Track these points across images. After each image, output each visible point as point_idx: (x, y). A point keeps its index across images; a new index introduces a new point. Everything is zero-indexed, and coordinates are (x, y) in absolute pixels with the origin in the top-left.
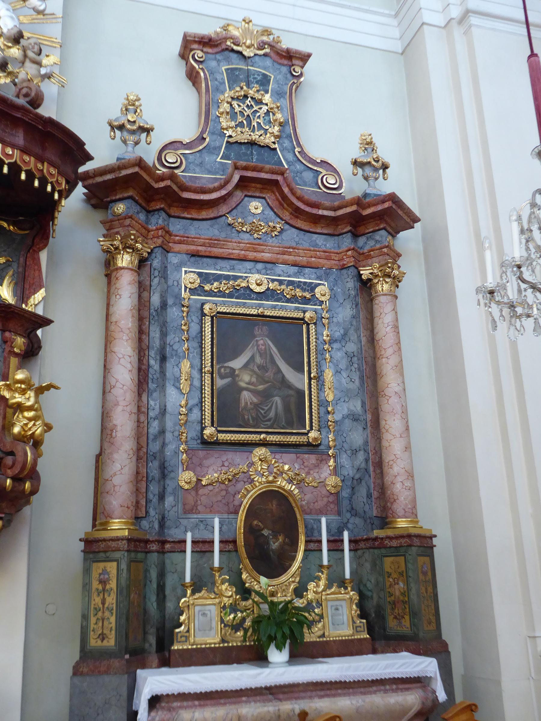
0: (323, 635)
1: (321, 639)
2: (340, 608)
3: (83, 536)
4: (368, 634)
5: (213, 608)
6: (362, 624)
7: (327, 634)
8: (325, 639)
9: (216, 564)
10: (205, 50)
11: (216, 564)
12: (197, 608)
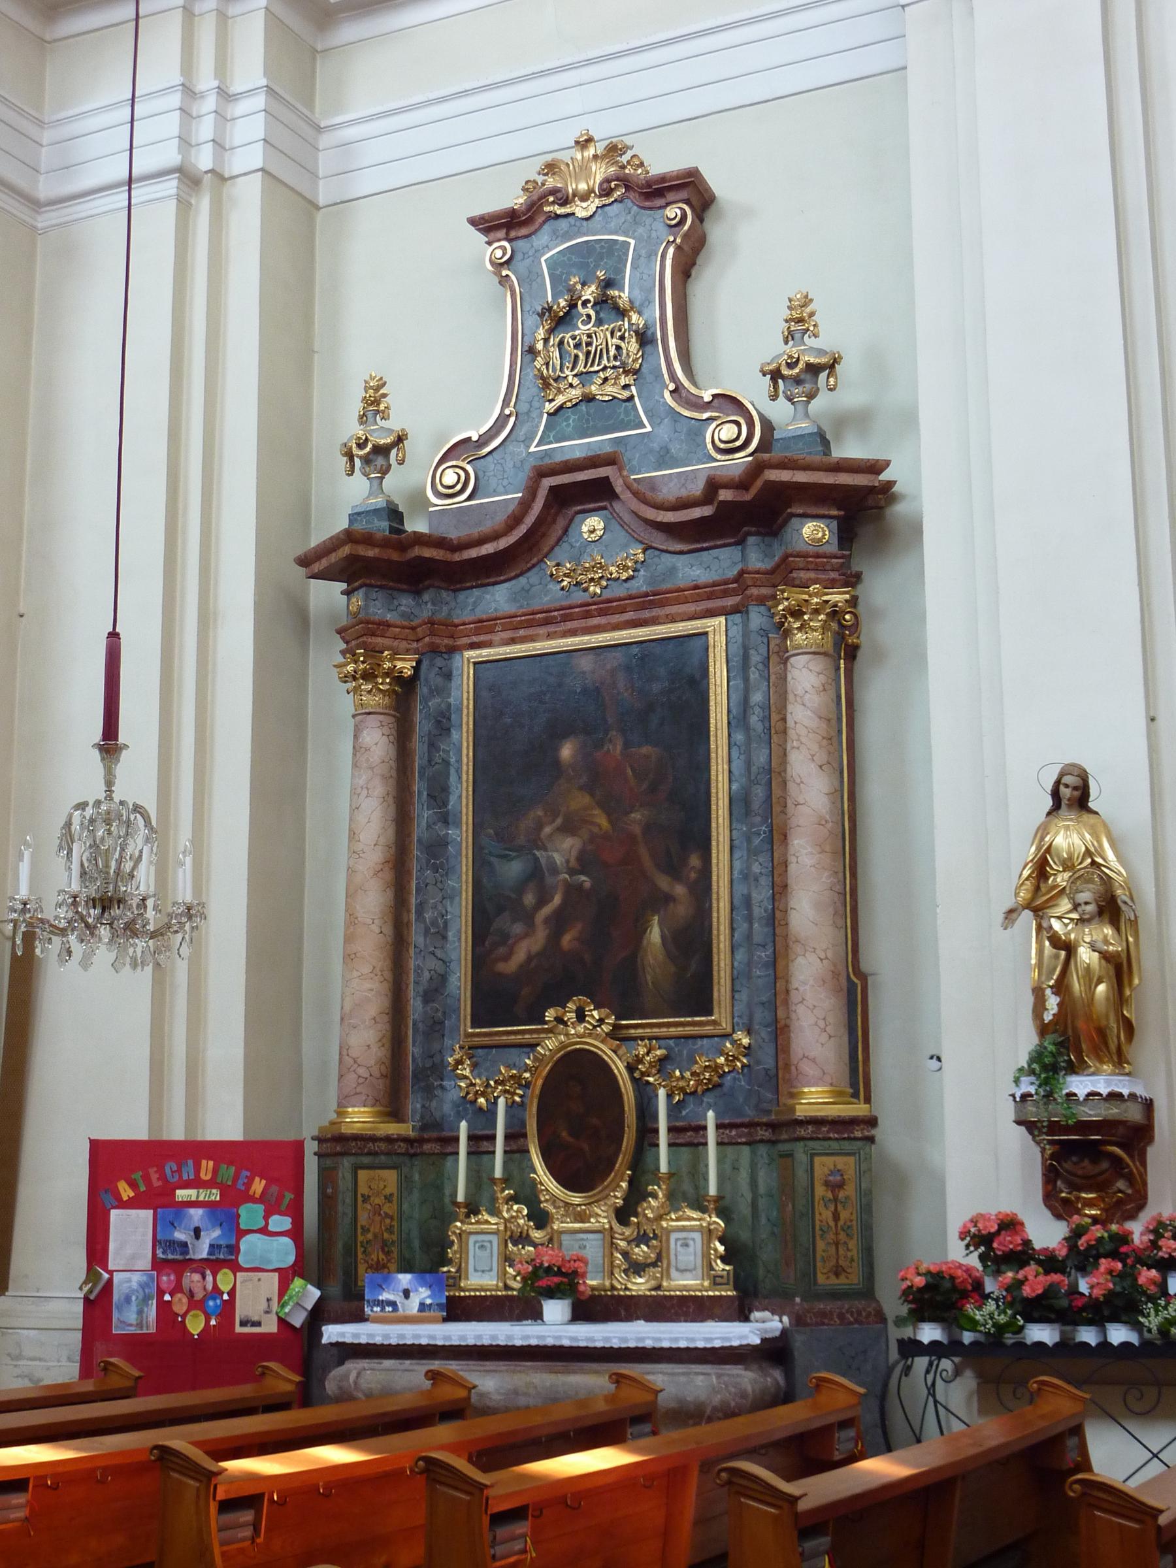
0: (658, 1287)
1: (653, 1293)
2: (691, 1243)
3: (316, 1133)
4: (735, 1289)
5: (494, 1239)
6: (725, 1273)
7: (665, 1284)
8: (661, 1293)
9: (498, 1173)
10: (513, 234)
11: (498, 1173)
12: (472, 1239)
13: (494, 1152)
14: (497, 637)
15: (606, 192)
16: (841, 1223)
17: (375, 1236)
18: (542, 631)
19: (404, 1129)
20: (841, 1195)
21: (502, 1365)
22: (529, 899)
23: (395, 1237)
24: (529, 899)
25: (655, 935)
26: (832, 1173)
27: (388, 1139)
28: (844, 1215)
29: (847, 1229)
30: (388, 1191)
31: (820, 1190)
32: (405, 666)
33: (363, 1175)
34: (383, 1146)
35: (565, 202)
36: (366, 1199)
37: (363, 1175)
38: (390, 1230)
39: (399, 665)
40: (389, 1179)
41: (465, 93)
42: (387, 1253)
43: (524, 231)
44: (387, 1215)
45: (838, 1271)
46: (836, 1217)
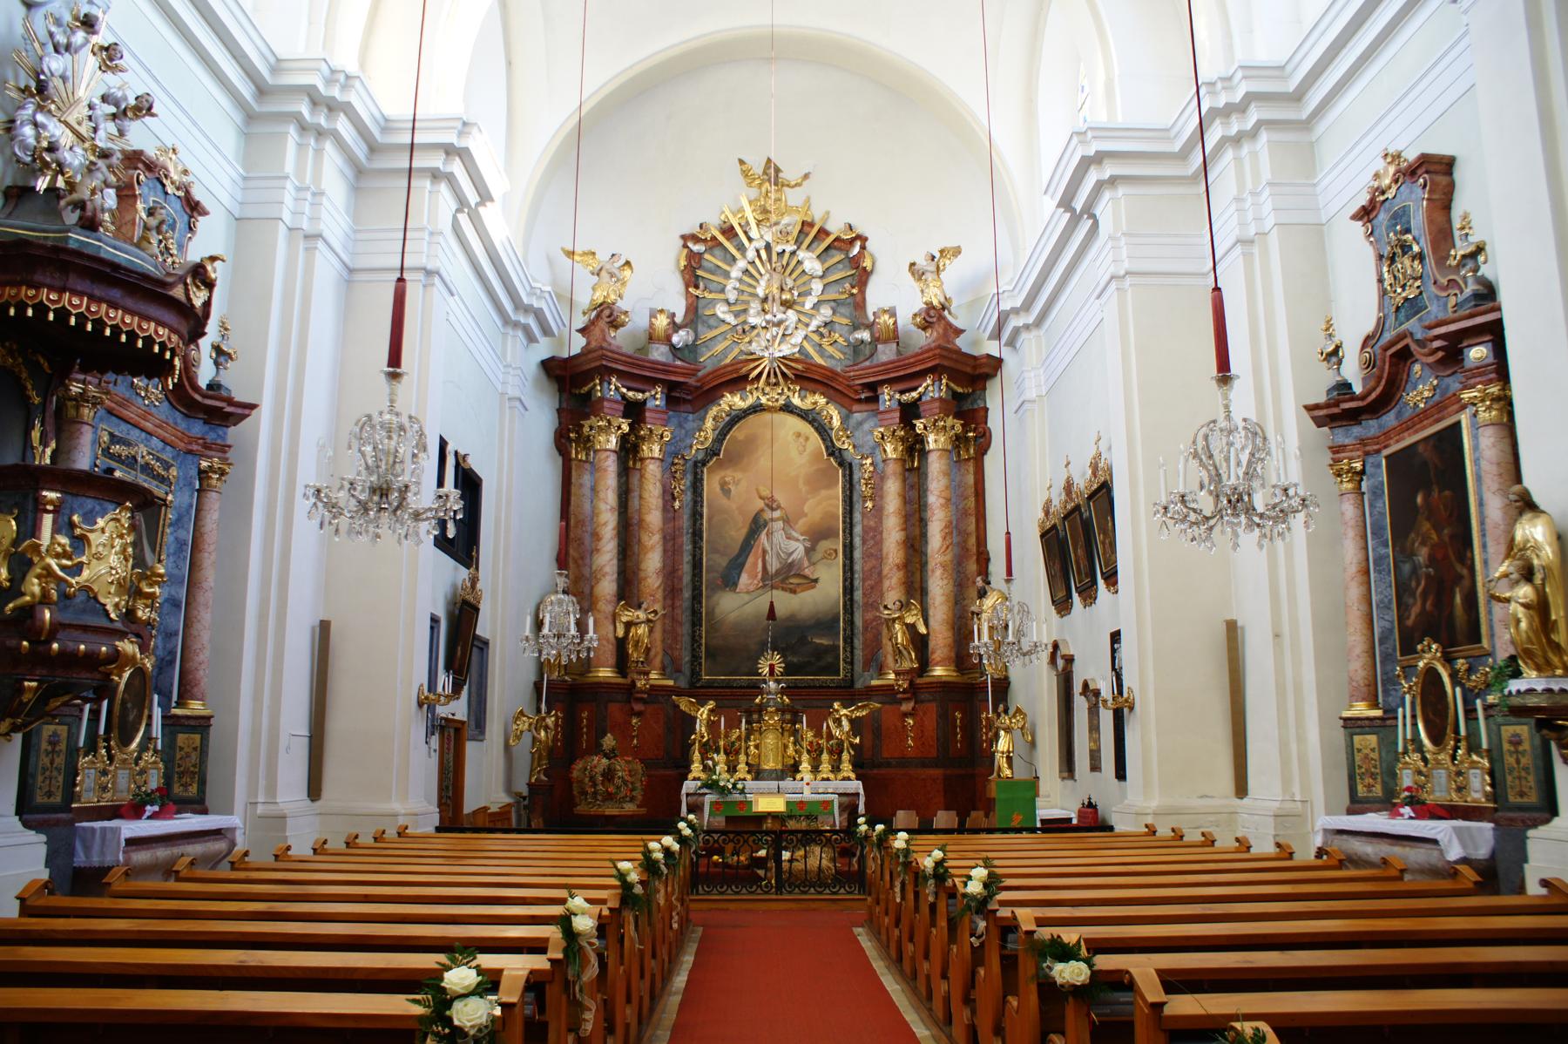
13: (1397, 726)
14: (1392, 442)
15: (1396, 181)
16: (1521, 765)
17: (1366, 770)
18: (1406, 434)
19: (1378, 713)
20: (1521, 748)
21: (1374, 840)
22: (1413, 584)
23: (1378, 771)
24: (1413, 584)
25: (1458, 599)
26: (1513, 736)
27: (1368, 719)
28: (1523, 761)
29: (1526, 769)
30: (1372, 746)
31: (1506, 746)
32: (1358, 465)
33: (1356, 738)
34: (1367, 722)
35: (1383, 193)
36: (1359, 750)
37: (1356, 738)
38: (1375, 767)
39: (1354, 465)
40: (1372, 740)
41: (1357, 143)
42: (1375, 779)
43: (1374, 214)
44: (1372, 759)
45: (1522, 794)
46: (1518, 762)
